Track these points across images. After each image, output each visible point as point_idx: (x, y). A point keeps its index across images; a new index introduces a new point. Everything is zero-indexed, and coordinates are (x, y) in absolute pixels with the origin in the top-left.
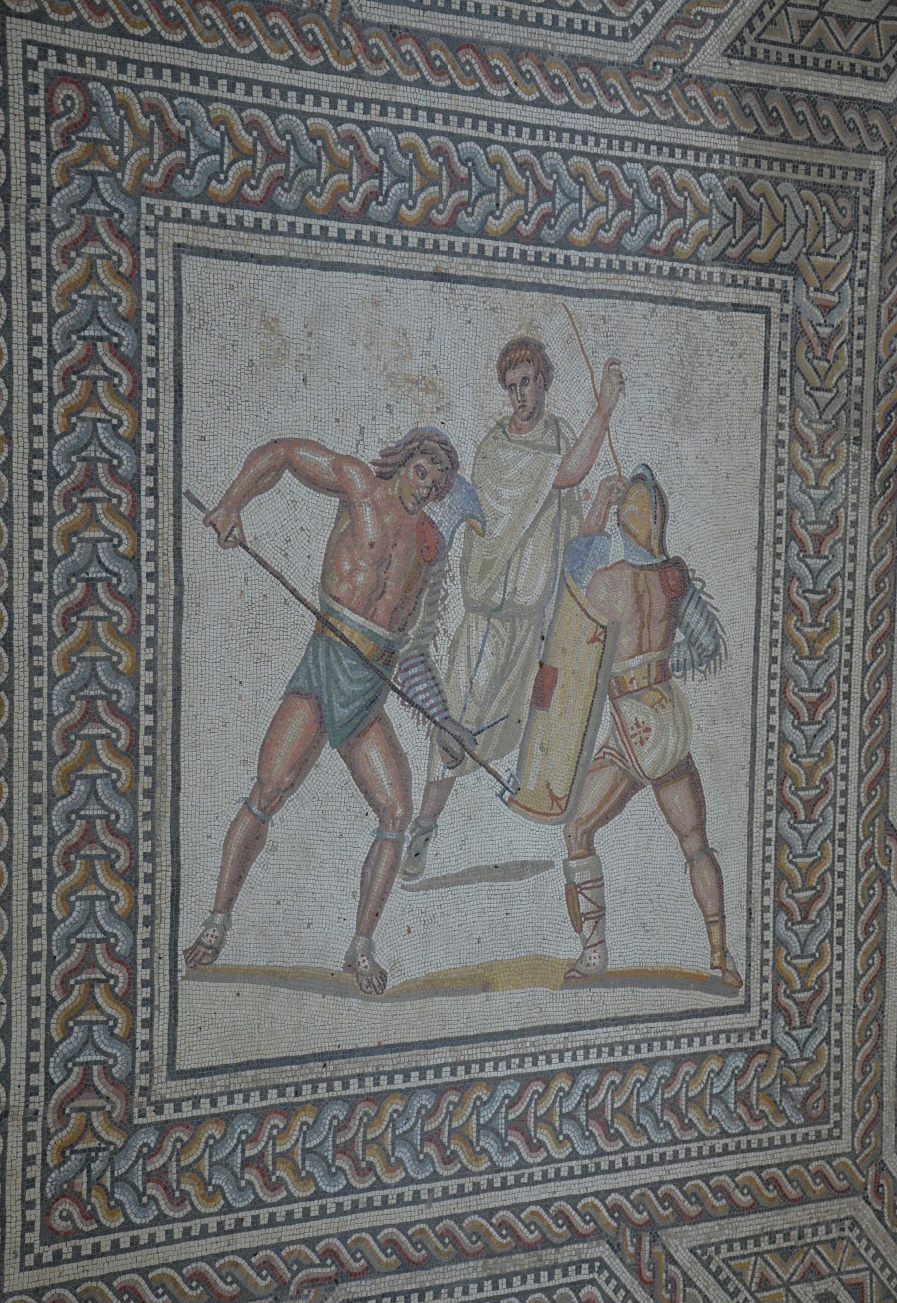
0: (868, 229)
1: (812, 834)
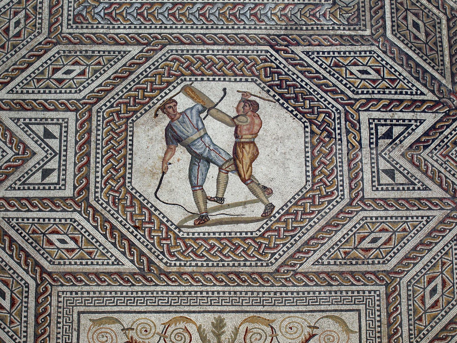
0: (349, 29)
1: (164, 16)
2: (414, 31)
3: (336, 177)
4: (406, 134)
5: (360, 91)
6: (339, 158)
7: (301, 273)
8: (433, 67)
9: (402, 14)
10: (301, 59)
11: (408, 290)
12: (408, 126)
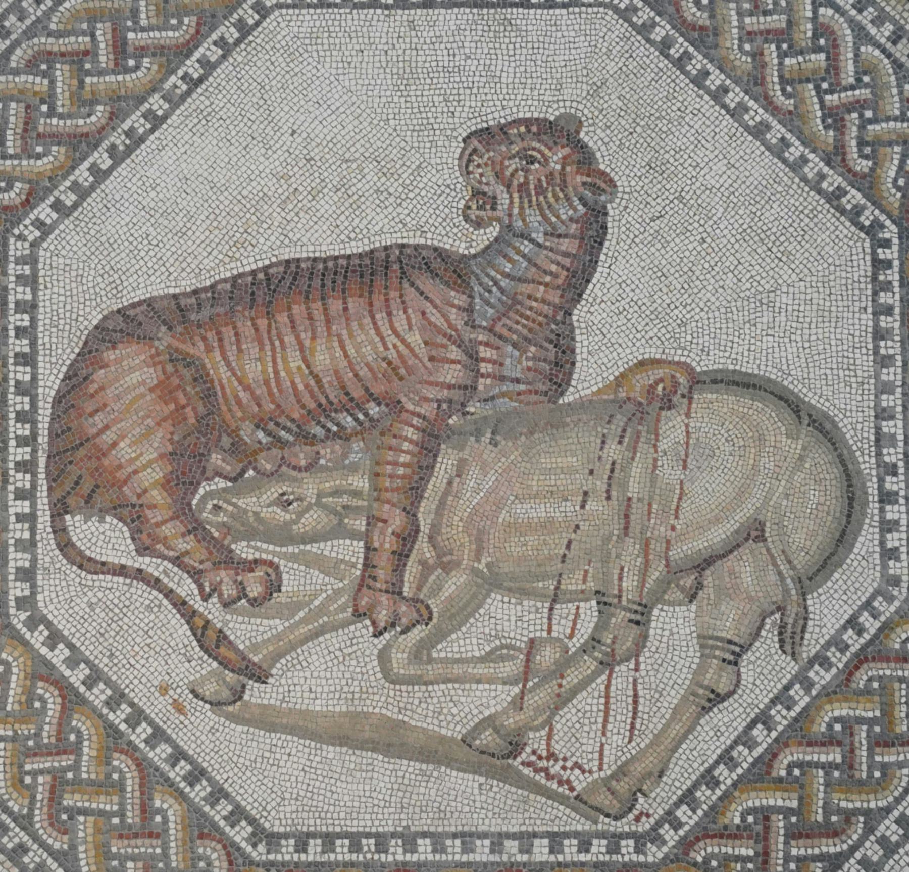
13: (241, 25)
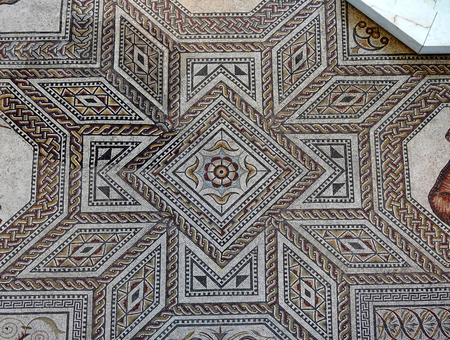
0: (81, 63)
2: (139, 63)
3: (58, 194)
4: (122, 155)
5: (85, 117)
6: (62, 177)
7: (19, 279)
8: (152, 95)
9: (129, 48)
10: (37, 90)
11: (113, 295)
12: (125, 148)
13: (405, 149)
